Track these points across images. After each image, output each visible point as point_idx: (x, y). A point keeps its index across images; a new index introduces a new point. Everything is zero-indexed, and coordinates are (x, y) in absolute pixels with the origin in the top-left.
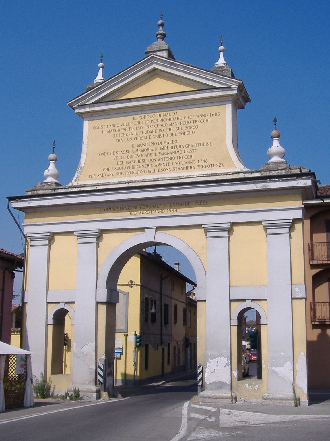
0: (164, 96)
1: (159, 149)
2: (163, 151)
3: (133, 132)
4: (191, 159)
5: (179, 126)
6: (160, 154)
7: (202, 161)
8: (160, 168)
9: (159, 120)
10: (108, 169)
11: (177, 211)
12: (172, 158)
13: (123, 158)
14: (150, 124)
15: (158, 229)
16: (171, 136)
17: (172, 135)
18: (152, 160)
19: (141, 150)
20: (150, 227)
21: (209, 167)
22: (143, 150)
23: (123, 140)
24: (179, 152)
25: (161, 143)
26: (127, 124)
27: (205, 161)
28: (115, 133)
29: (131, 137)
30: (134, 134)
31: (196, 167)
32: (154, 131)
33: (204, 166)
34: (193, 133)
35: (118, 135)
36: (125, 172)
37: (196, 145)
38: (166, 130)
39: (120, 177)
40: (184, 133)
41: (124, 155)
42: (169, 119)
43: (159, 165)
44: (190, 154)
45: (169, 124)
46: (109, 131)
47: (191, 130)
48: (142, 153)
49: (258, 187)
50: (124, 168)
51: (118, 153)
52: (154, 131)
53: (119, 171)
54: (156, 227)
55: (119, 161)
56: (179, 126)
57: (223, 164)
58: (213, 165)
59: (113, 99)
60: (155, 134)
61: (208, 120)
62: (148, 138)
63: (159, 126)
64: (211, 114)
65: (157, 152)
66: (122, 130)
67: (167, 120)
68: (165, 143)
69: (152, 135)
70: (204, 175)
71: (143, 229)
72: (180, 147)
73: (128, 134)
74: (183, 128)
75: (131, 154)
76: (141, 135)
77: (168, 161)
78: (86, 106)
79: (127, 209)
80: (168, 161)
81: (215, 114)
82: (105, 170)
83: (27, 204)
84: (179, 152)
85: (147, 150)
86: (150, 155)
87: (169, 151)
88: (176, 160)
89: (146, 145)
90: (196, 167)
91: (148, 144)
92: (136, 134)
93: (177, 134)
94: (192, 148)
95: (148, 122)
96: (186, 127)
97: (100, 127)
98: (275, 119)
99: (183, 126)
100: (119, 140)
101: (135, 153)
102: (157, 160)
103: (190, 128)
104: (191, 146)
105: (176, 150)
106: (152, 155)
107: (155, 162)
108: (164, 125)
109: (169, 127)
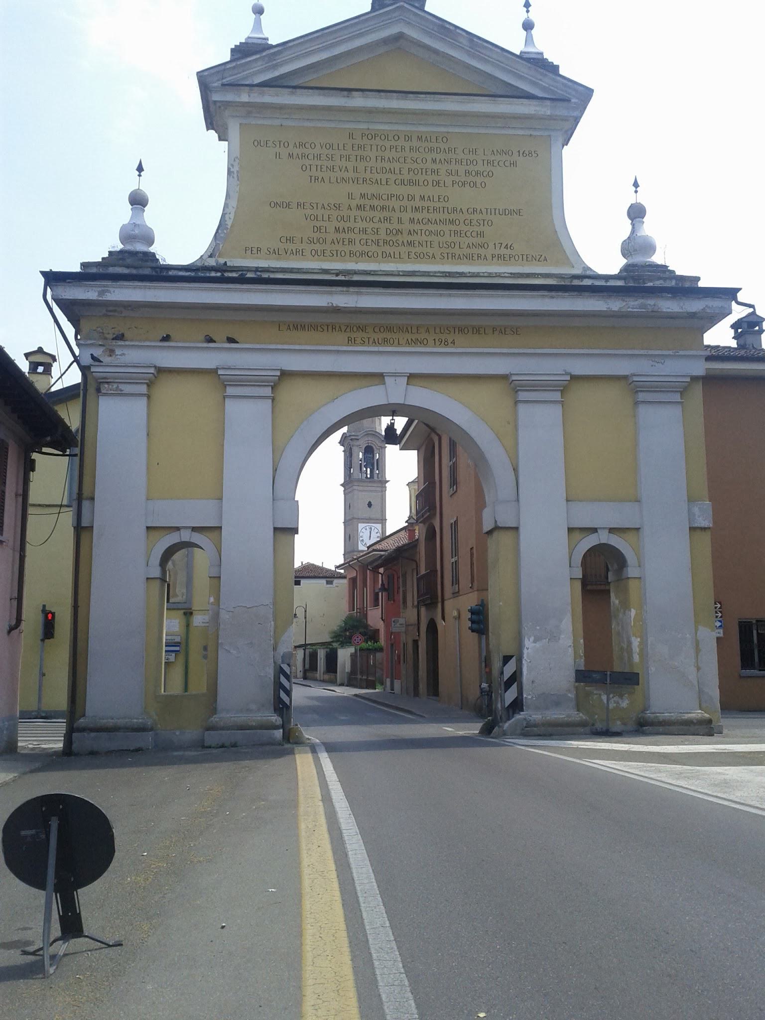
0: (428, 96)
1: (409, 209)
2: (418, 216)
3: (350, 165)
4: (479, 240)
5: (453, 167)
6: (412, 221)
7: (503, 246)
8: (413, 250)
9: (407, 149)
10: (290, 240)
11: (454, 343)
12: (437, 234)
13: (326, 218)
14: (387, 154)
15: (412, 378)
16: (434, 185)
17: (438, 183)
18: (394, 231)
19: (368, 208)
20: (396, 373)
21: (517, 259)
22: (372, 208)
23: (327, 180)
24: (452, 222)
25: (413, 198)
26: (335, 147)
27: (509, 246)
28: (307, 162)
29: (346, 175)
30: (350, 169)
31: (489, 257)
32: (397, 171)
33: (507, 258)
34: (484, 185)
35: (313, 168)
36: (333, 251)
37: (489, 210)
38: (424, 171)
39: (321, 261)
40: (464, 184)
41: (329, 212)
42: (431, 150)
43: (410, 243)
44: (476, 229)
45: (429, 160)
46: (291, 156)
47: (479, 180)
48: (372, 214)
49: (632, 308)
50: (329, 241)
51: (315, 206)
52: (397, 171)
53: (317, 247)
54: (410, 374)
55: (318, 224)
56: (453, 167)
57: (545, 257)
58: (525, 257)
59: (305, 82)
60: (400, 177)
61: (514, 164)
62: (384, 182)
63: (408, 160)
64: (519, 152)
65: (406, 217)
66: (324, 157)
67: (427, 150)
68: (422, 198)
69: (392, 177)
70: (511, 274)
71: (378, 377)
72: (455, 212)
73: (336, 169)
74: (461, 172)
75: (345, 212)
76: (368, 175)
77: (429, 239)
78: (242, 88)
79: (343, 330)
80: (429, 239)
81: (528, 154)
82: (283, 240)
83: (97, 294)
84: (452, 222)
85: (383, 208)
86: (388, 220)
87: (432, 216)
88: (447, 238)
89: (380, 197)
90: (489, 257)
91: (385, 197)
92: (355, 170)
93: (449, 182)
94: (480, 217)
95: (383, 148)
96: (467, 171)
97: (270, 144)
98: (636, 182)
99: (462, 169)
100: (316, 179)
101: (354, 212)
102: (405, 233)
103: (477, 173)
104: (434, 223)
105: (446, 216)
106: (395, 220)
107: (399, 237)
108: (419, 161)
109: (430, 165)
